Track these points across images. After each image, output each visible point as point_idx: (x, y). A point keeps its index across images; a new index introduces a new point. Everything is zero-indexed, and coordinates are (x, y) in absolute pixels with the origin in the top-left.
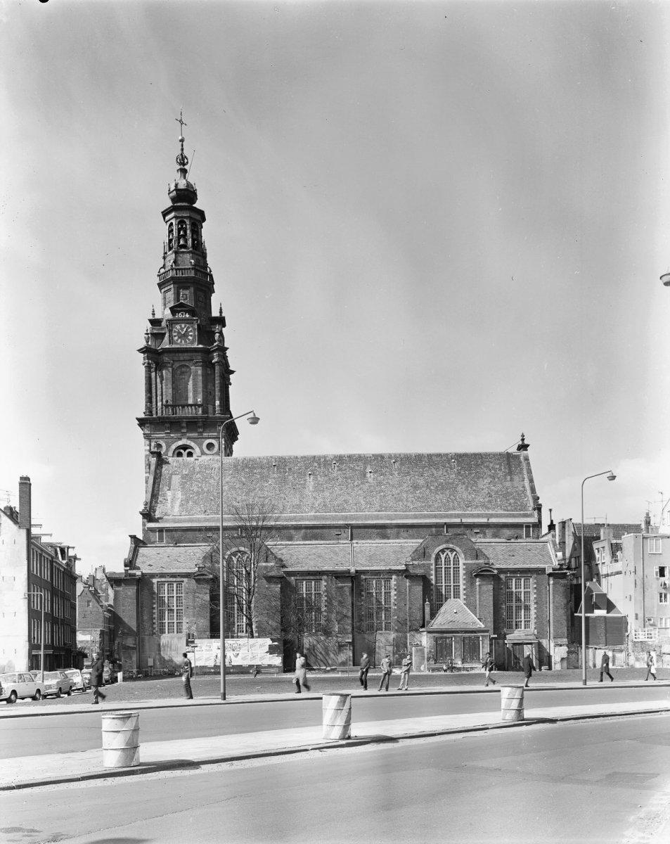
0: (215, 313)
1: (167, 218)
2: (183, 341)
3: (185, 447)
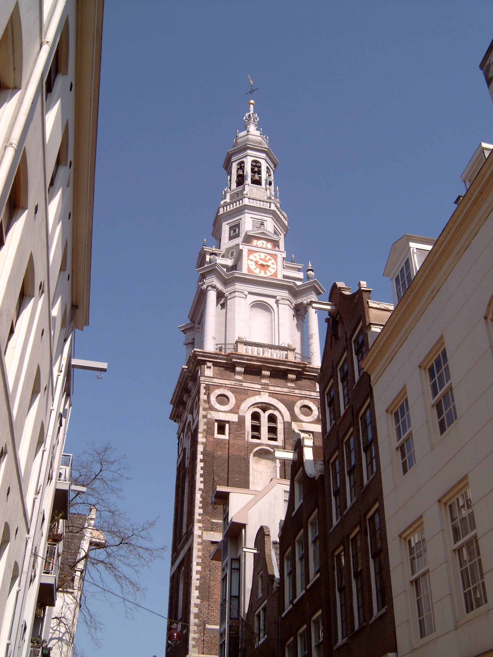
1: (233, 159)
3: (265, 407)
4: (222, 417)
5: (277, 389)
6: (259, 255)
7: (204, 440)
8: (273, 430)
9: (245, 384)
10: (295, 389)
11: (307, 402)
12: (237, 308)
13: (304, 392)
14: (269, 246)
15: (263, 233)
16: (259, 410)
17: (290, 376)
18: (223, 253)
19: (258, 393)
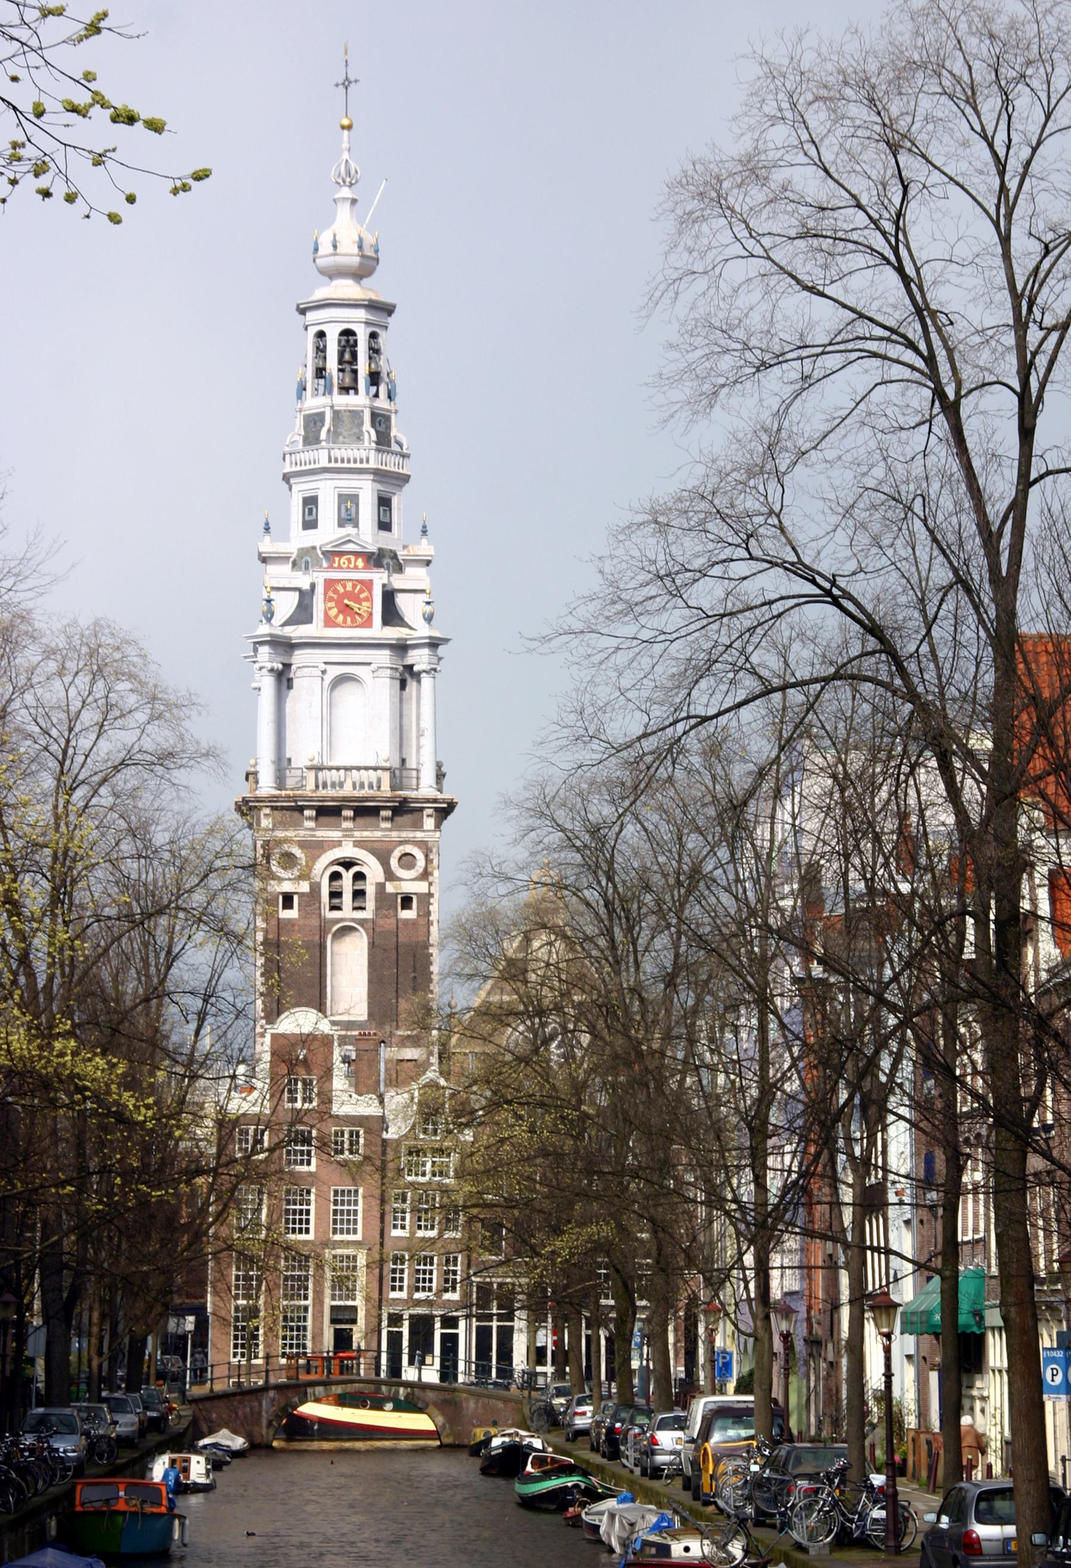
3: (348, 864)
4: (287, 887)
5: (365, 834)
6: (344, 587)
7: (264, 926)
8: (359, 894)
9: (319, 833)
11: (409, 849)
14: (360, 563)
16: (340, 869)
17: (383, 813)
19: (339, 844)
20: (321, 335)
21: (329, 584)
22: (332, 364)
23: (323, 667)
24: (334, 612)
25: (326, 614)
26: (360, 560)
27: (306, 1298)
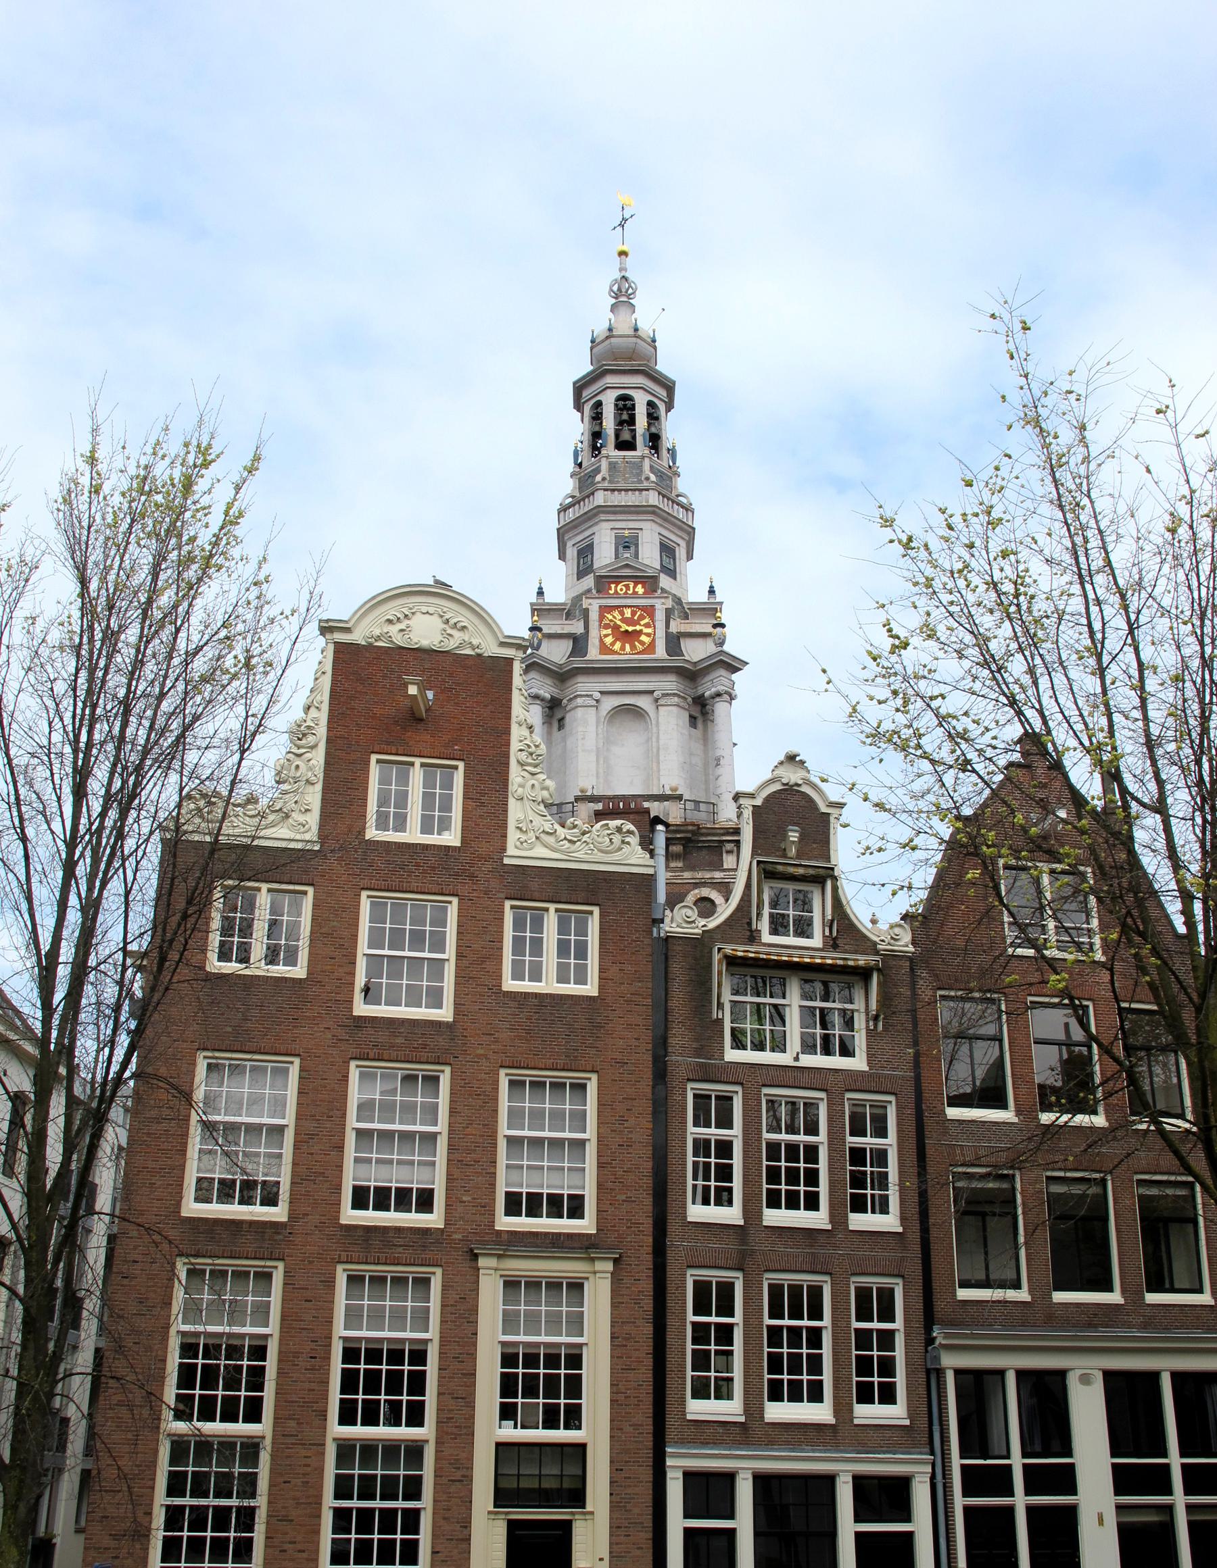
0: (696, 594)
1: (586, 393)
2: (628, 647)
6: (622, 614)
10: (682, 871)
11: (705, 892)
12: (580, 729)
13: (700, 875)
14: (640, 589)
15: (627, 566)
18: (568, 607)
20: (599, 404)
21: (604, 610)
22: (609, 423)
23: (597, 695)
24: (609, 640)
25: (601, 640)
26: (640, 586)
27: (416, 1418)
